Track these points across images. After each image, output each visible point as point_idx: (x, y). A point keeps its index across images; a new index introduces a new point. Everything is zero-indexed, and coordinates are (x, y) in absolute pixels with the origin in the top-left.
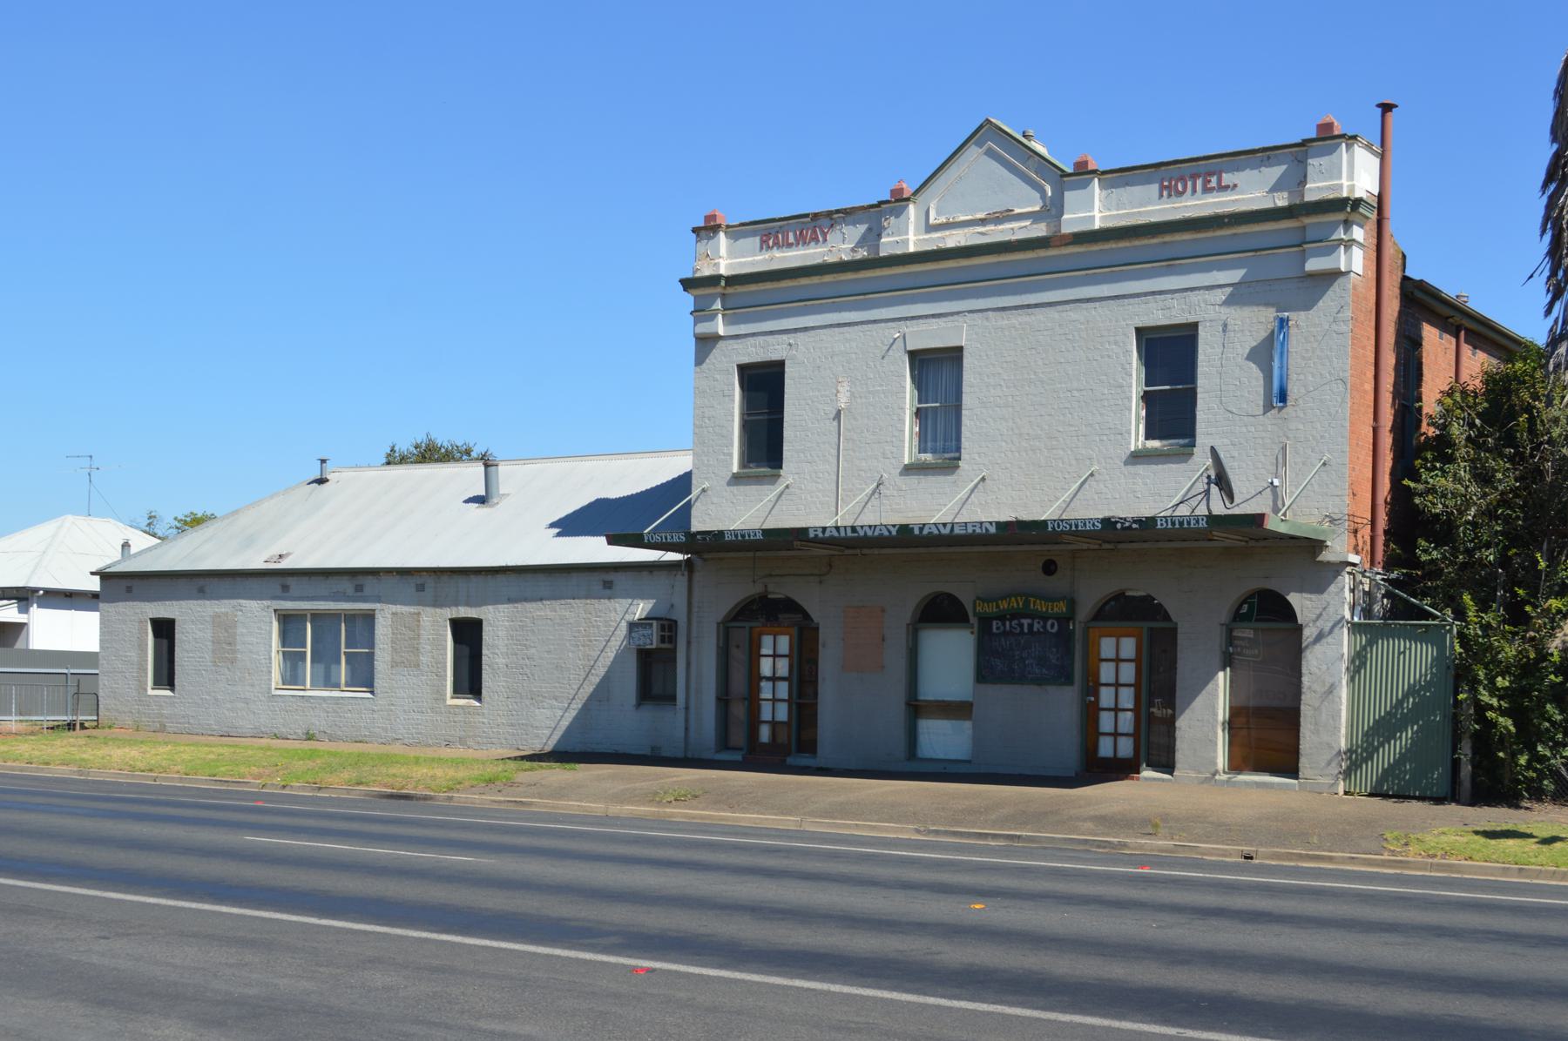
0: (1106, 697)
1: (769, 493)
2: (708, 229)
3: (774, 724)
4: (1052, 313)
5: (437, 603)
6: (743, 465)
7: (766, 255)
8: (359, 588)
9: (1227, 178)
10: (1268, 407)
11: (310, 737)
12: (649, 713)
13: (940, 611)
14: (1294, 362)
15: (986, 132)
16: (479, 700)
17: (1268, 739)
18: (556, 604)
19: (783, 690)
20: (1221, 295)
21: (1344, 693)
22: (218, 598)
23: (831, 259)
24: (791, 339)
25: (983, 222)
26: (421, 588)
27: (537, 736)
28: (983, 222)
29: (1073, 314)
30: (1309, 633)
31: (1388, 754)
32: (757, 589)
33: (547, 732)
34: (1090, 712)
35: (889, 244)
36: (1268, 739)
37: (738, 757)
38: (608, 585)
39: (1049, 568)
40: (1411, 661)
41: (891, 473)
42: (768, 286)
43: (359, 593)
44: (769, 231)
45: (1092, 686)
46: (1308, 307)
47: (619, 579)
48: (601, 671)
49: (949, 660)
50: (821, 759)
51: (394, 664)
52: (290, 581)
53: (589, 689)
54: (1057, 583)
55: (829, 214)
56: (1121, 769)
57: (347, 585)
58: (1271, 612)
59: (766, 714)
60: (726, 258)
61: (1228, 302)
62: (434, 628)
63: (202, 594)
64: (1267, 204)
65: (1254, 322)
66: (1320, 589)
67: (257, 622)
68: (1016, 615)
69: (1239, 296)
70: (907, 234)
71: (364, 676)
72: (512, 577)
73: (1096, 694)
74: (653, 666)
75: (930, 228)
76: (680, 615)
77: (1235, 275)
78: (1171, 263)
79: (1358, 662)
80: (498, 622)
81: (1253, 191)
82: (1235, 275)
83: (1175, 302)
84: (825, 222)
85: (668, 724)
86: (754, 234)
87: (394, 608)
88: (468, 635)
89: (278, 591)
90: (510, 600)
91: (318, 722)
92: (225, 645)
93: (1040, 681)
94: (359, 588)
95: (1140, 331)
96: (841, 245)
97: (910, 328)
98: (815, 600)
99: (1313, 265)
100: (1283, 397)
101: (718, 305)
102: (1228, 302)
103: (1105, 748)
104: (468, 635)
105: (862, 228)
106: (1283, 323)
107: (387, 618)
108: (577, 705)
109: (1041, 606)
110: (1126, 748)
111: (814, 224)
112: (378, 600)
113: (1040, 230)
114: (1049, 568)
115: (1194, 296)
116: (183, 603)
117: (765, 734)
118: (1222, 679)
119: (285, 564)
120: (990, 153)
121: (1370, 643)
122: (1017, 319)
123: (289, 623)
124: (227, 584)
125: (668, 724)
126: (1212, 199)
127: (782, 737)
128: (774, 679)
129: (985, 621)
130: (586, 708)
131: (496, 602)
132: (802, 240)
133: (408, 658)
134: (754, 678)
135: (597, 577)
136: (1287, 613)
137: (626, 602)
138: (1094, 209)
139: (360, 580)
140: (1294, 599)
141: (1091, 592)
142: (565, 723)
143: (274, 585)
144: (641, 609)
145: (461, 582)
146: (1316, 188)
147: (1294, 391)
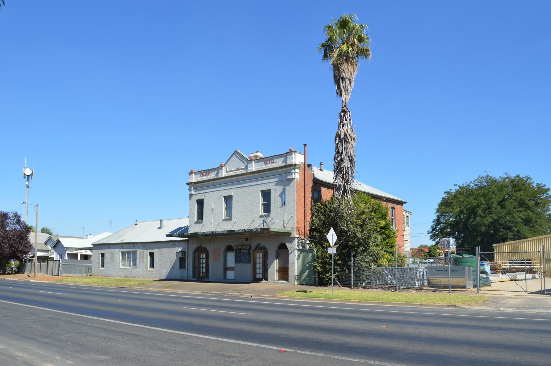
0: (257, 265)
1: (201, 225)
2: (191, 173)
3: (203, 272)
4: (247, 188)
5: (147, 249)
6: (197, 220)
8: (134, 246)
9: (275, 160)
10: (282, 206)
11: (126, 277)
12: (181, 271)
13: (229, 249)
14: (286, 196)
15: (236, 153)
17: (284, 273)
20: (274, 184)
21: (296, 264)
25: (235, 170)
26: (144, 246)
28: (235, 170)
29: (250, 188)
30: (290, 251)
31: (304, 276)
32: (199, 245)
34: (255, 269)
35: (220, 175)
36: (284, 273)
39: (247, 239)
40: (308, 257)
41: (221, 221)
44: (201, 173)
45: (255, 263)
47: (111, 246)
48: (173, 262)
51: (140, 262)
52: (123, 245)
53: (171, 266)
54: (248, 243)
56: (259, 280)
57: (132, 246)
58: (283, 248)
60: (194, 179)
62: (146, 253)
63: (109, 248)
65: (279, 189)
66: (291, 243)
67: (118, 252)
68: (241, 249)
69: (278, 183)
71: (135, 264)
72: (139, 244)
73: (256, 265)
74: (182, 260)
75: (227, 172)
76: (186, 251)
77: (276, 180)
78: (266, 178)
79: (299, 257)
80: (156, 252)
81: (279, 163)
82: (276, 180)
83: (267, 185)
85: (184, 273)
88: (152, 255)
90: (159, 248)
91: (127, 273)
92: (112, 258)
93: (245, 263)
94: (134, 246)
95: (262, 191)
96: (212, 176)
97: (224, 192)
98: (209, 247)
99: (289, 177)
100: (285, 204)
103: (257, 277)
104: (152, 255)
106: (284, 189)
107: (139, 252)
108: (169, 269)
109: (244, 247)
110: (261, 276)
111: (209, 171)
112: (137, 248)
113: (244, 172)
114: (247, 239)
115: (270, 184)
118: (276, 261)
119: (123, 242)
120: (237, 157)
121: (301, 253)
122: (241, 189)
123: (123, 253)
125: (184, 273)
128: (203, 263)
129: (236, 250)
131: (156, 249)
132: (206, 175)
134: (200, 263)
135: (173, 243)
136: (286, 248)
138: (253, 167)
140: (287, 244)
141: (254, 244)
143: (120, 246)
144: (180, 249)
145: (151, 245)
146: (289, 162)
147: (286, 202)
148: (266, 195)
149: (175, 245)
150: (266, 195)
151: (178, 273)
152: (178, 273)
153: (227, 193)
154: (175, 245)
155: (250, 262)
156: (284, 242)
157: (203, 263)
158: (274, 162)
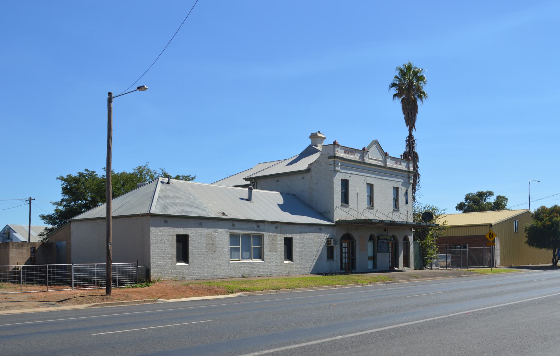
3: (345, 263)
5: (281, 233)
7: (345, 155)
8: (258, 227)
11: (243, 277)
15: (376, 142)
20: (401, 183)
22: (208, 228)
26: (276, 228)
29: (387, 182)
32: (345, 232)
37: (344, 271)
39: (385, 230)
43: (258, 228)
48: (320, 252)
50: (357, 271)
51: (270, 251)
52: (236, 223)
53: (318, 257)
55: (356, 150)
57: (254, 225)
58: (406, 239)
59: (344, 261)
60: (340, 153)
62: (280, 239)
63: (201, 225)
67: (222, 236)
71: (260, 255)
74: (329, 250)
78: (396, 176)
80: (297, 239)
82: (402, 181)
87: (269, 234)
88: (288, 242)
89: (231, 226)
90: (300, 233)
91: (246, 271)
92: (211, 244)
93: (385, 252)
94: (258, 227)
96: (356, 157)
97: (367, 178)
98: (356, 235)
104: (288, 242)
106: (407, 191)
108: (315, 261)
112: (264, 231)
113: (382, 165)
116: (193, 229)
123: (234, 238)
127: (347, 266)
128: (345, 253)
130: (317, 262)
133: (273, 249)
139: (259, 224)
142: (313, 266)
143: (230, 224)
145: (287, 227)
148: (396, 190)
149: (320, 229)
150: (396, 190)
151: (326, 264)
152: (326, 264)
153: (370, 181)
154: (320, 229)
155: (388, 251)
157: (345, 253)
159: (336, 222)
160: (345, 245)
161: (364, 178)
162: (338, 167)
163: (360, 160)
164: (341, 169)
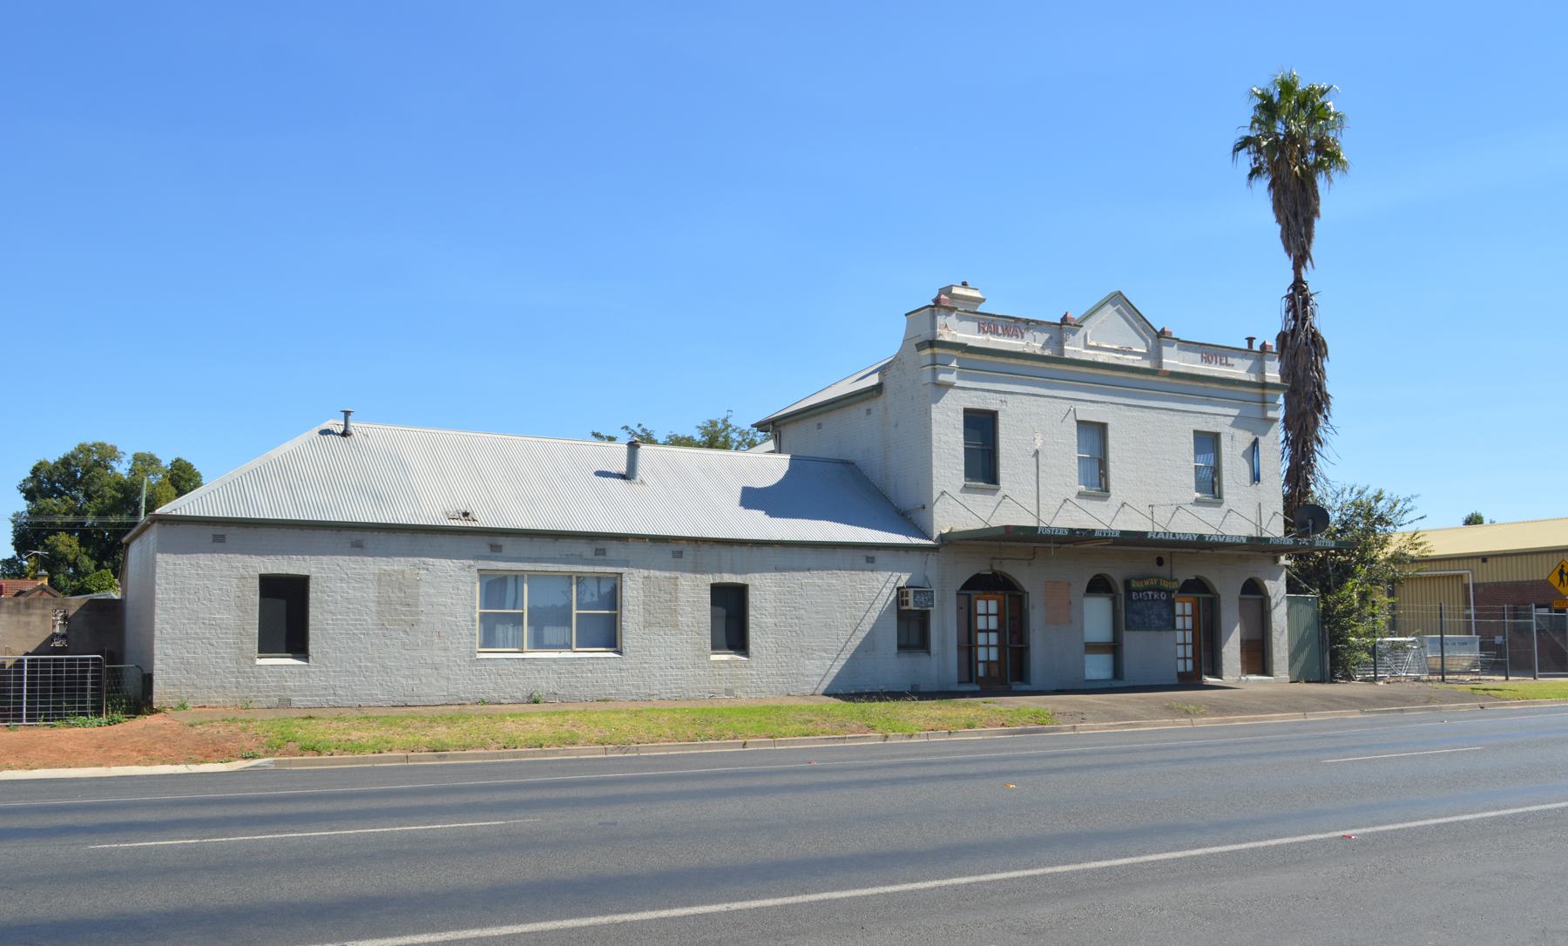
3: (988, 663)
5: (696, 569)
9: (1230, 360)
13: (1099, 586)
15: (1118, 299)
16: (306, 658)
18: (824, 574)
19: (993, 638)
20: (1230, 420)
22: (388, 555)
23: (1028, 350)
24: (1003, 397)
27: (808, 683)
29: (1164, 416)
30: (1273, 602)
33: (818, 679)
36: (1257, 658)
37: (977, 688)
38: (870, 560)
39: (1160, 562)
40: (1307, 614)
41: (1072, 497)
42: (989, 358)
43: (600, 555)
46: (1264, 434)
48: (866, 627)
49: (1096, 617)
50: (1033, 687)
52: (501, 540)
53: (856, 642)
54: (1164, 571)
55: (1027, 321)
57: (586, 549)
58: (1254, 589)
59: (982, 654)
60: (955, 330)
61: (1233, 425)
62: (693, 593)
63: (358, 548)
64: (1247, 378)
69: (1238, 423)
70: (1073, 349)
71: (609, 636)
74: (911, 623)
77: (1235, 412)
78: (1208, 399)
82: (1235, 412)
83: (1210, 418)
84: (1023, 326)
86: (973, 320)
87: (645, 573)
89: (486, 551)
90: (777, 569)
91: (544, 684)
92: (400, 610)
93: (1159, 629)
96: (1033, 343)
97: (1079, 406)
98: (1025, 576)
101: (954, 364)
102: (1233, 425)
105: (1046, 336)
106: (1255, 443)
108: (845, 656)
112: (626, 564)
113: (1146, 364)
114: (1160, 562)
115: (1219, 418)
116: (325, 559)
117: (981, 671)
120: (1118, 311)
122: (1135, 413)
123: (495, 588)
124: (403, 539)
126: (1224, 369)
127: (995, 672)
128: (987, 631)
130: (853, 657)
131: (753, 571)
132: (1007, 332)
133: (663, 616)
137: (887, 574)
138: (1173, 360)
139: (601, 544)
140: (1267, 583)
141: (1184, 574)
142: (835, 671)
144: (904, 579)
145: (725, 552)
148: (1208, 442)
150: (1208, 442)
151: (893, 666)
152: (893, 666)
153: (1092, 412)
156: (1258, 576)
157: (987, 631)
158: (1227, 365)
159: (942, 536)
160: (987, 609)
161: (1066, 405)
162: (951, 371)
163: (1047, 353)
164: (960, 377)
